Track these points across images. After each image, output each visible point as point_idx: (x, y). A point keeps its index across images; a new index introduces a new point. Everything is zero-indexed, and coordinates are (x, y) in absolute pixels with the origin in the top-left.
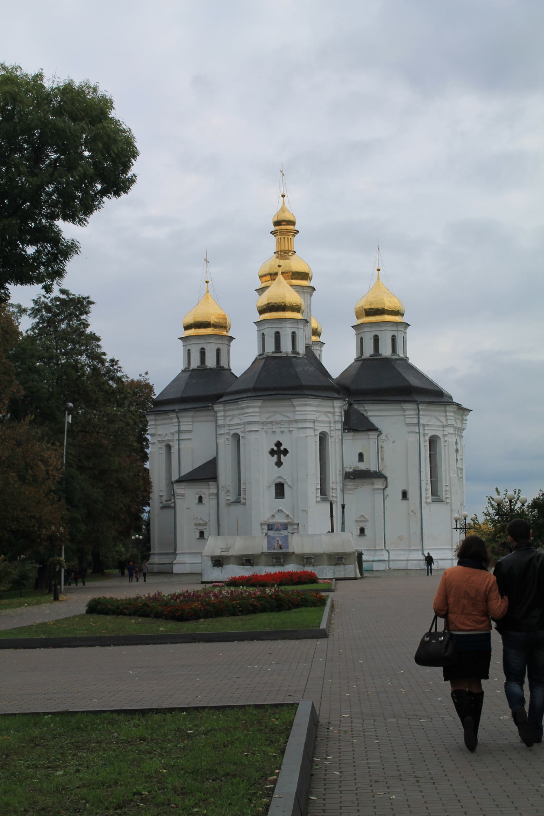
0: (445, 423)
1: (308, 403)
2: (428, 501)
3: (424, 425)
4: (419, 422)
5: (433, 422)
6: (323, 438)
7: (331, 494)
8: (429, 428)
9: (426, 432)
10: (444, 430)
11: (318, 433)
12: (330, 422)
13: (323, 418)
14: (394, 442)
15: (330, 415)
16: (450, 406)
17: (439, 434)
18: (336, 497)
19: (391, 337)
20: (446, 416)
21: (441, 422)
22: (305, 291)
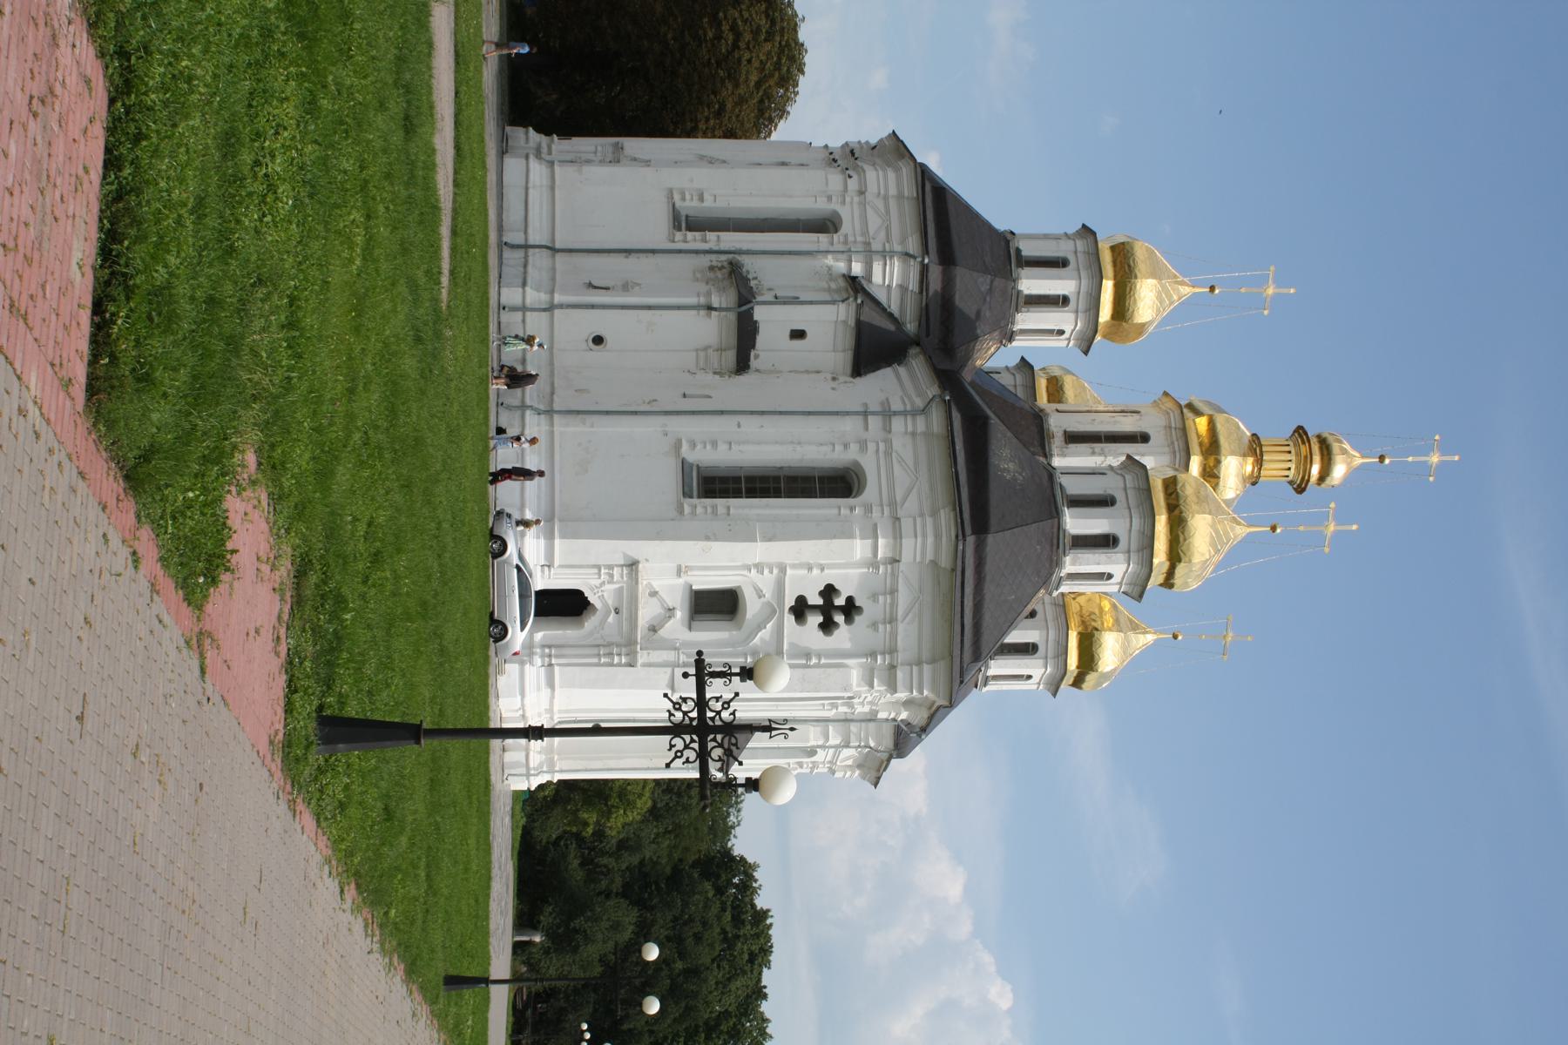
0: (900, 513)
1: (904, 170)
2: (685, 447)
3: (888, 442)
4: (895, 413)
5: (902, 478)
6: (826, 225)
7: (690, 235)
8: (881, 455)
9: (871, 446)
10: (882, 505)
11: (835, 206)
12: (865, 232)
13: (874, 222)
14: (833, 389)
15: (882, 234)
16: (952, 514)
17: (870, 493)
18: (685, 241)
19: (1110, 492)
20: (922, 515)
21: (905, 499)
22: (1176, 443)
